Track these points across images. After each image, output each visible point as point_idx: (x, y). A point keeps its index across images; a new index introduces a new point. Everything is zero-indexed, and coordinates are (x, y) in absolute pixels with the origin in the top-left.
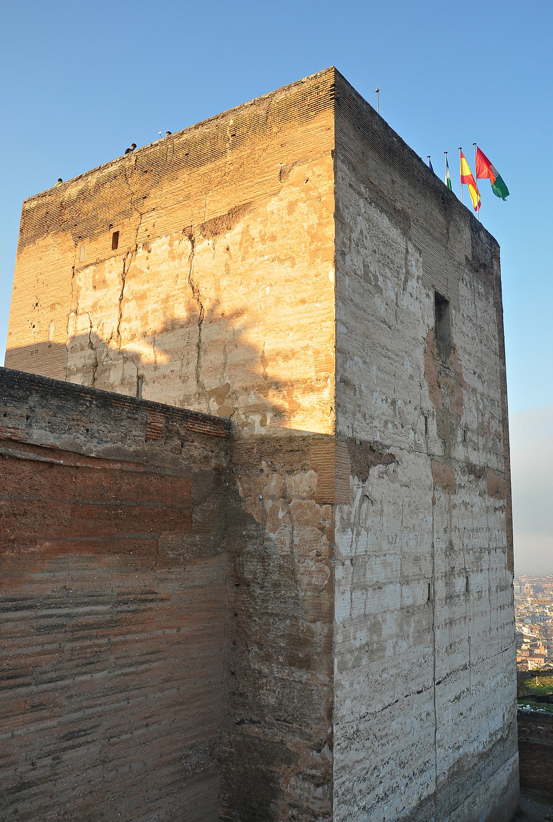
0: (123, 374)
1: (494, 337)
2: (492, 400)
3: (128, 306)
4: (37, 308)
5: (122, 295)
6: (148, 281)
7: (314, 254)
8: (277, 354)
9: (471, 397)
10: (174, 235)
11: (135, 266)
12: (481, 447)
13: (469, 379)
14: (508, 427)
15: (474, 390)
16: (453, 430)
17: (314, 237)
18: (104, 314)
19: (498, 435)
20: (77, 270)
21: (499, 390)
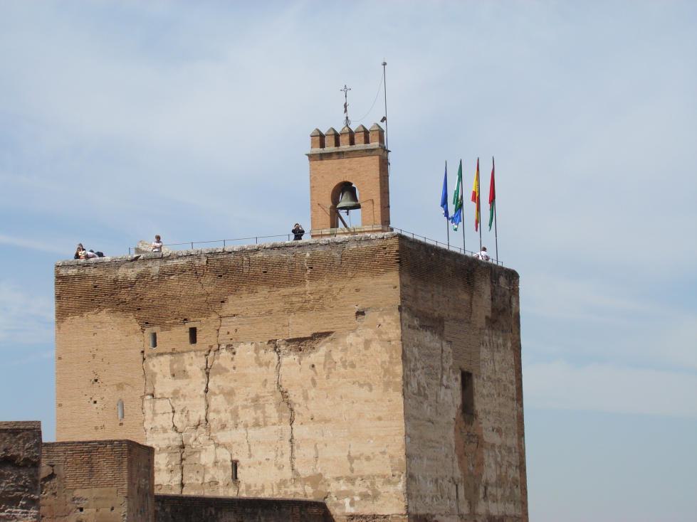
0: (216, 457)
1: (511, 382)
2: (510, 448)
3: (215, 399)
4: (96, 383)
5: (207, 388)
6: (235, 381)
7: (387, 385)
8: (362, 455)
9: (491, 454)
10: (259, 344)
11: (219, 364)
12: (499, 498)
13: (490, 437)
14: (525, 470)
15: (493, 446)
16: (476, 490)
17: (387, 371)
18: (187, 402)
19: (515, 482)
20: (149, 356)
21: (517, 435)
